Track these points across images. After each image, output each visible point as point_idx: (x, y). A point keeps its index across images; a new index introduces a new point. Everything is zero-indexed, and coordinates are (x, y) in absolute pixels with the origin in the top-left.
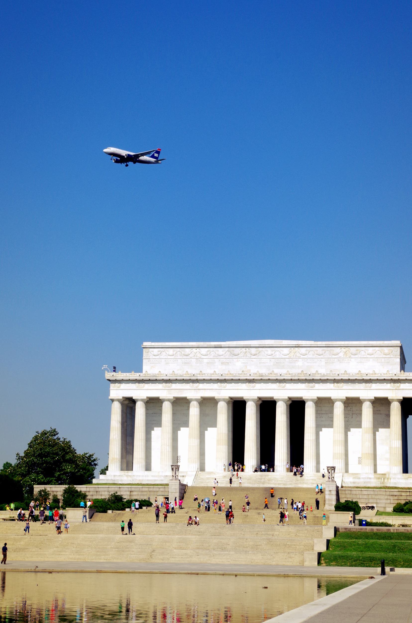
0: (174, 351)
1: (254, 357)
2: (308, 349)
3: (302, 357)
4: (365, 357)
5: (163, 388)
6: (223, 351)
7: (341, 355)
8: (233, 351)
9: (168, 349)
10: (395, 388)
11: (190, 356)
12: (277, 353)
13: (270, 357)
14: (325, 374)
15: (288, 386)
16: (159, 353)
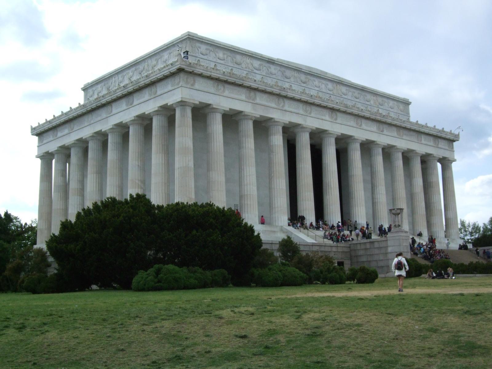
0: (224, 54)
1: (304, 85)
2: (348, 88)
3: (344, 96)
4: (388, 109)
5: (247, 100)
6: (275, 69)
7: (372, 102)
8: (285, 72)
9: (217, 50)
10: (436, 146)
11: (243, 66)
12: (323, 86)
13: (317, 89)
14: (395, 119)
15: (365, 125)
16: (208, 51)
